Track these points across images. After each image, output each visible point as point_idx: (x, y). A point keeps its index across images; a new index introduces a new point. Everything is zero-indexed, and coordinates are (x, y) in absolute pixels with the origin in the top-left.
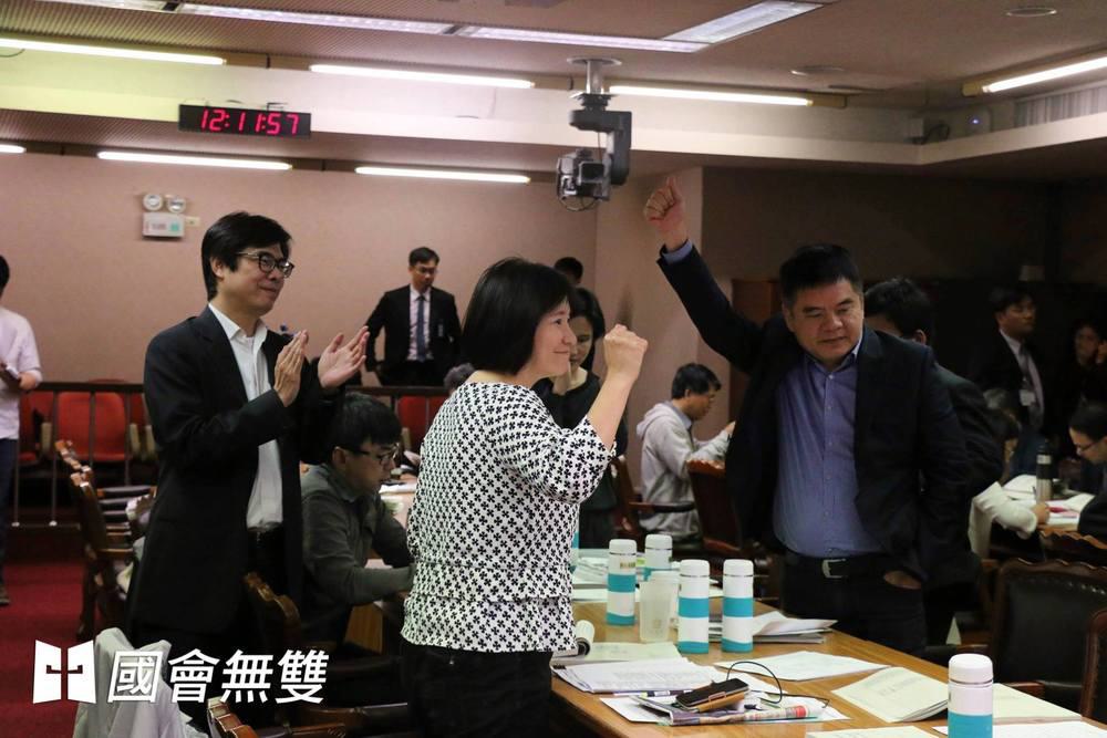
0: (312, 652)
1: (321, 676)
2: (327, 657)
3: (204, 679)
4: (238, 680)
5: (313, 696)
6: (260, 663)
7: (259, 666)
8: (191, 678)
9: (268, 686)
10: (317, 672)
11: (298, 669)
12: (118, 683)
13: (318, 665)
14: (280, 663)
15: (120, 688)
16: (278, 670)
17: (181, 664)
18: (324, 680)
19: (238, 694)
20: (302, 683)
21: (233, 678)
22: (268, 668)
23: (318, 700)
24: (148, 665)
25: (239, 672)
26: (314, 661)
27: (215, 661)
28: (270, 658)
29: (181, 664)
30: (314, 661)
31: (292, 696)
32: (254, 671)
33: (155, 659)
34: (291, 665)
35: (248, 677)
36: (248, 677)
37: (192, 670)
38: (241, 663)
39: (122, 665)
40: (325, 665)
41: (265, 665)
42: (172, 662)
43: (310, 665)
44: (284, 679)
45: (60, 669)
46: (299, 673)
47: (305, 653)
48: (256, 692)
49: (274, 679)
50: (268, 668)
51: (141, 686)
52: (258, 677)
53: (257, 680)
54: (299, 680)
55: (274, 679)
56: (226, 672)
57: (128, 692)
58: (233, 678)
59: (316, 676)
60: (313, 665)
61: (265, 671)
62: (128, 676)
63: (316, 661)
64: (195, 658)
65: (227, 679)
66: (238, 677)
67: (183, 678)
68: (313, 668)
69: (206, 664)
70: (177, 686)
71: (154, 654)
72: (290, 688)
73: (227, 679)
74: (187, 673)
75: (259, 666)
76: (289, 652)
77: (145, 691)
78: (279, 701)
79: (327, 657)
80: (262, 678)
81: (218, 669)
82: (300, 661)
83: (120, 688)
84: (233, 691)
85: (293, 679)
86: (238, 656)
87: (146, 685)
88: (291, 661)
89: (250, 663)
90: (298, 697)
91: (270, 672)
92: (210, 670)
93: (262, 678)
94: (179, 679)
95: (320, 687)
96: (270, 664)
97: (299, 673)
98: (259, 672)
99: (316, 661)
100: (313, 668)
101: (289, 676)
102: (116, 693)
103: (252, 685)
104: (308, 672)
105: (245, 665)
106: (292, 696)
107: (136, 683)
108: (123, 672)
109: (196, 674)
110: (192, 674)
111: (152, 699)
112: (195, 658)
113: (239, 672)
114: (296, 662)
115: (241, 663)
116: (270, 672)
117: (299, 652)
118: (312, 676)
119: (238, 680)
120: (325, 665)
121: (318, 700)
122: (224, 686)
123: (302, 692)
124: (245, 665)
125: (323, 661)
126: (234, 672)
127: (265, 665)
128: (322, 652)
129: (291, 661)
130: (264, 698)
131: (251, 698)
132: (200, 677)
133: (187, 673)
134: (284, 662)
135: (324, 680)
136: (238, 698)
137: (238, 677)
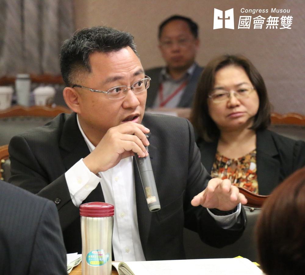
0: (289, 16)
1: (291, 22)
2: (292, 18)
3: (262, 23)
5: (289, 27)
6: (276, 19)
7: (276, 20)
8: (259, 23)
9: (278, 25)
10: (290, 21)
11: (285, 20)
12: (240, 24)
13: (290, 19)
14: (281, 19)
15: (241, 25)
16: (280, 21)
18: (292, 23)
19: (270, 27)
20: (286, 24)
21: (269, 23)
22: (278, 20)
23: (290, 28)
25: (271, 21)
26: (289, 18)
27: (265, 18)
28: (278, 18)
29: (256, 19)
30: (289, 18)
31: (284, 27)
32: (274, 21)
34: (283, 20)
35: (273, 22)
36: (273, 22)
37: (259, 21)
38: (271, 19)
40: (292, 19)
41: (277, 19)
42: (254, 19)
43: (288, 19)
44: (282, 23)
45: (225, 20)
46: (286, 21)
48: (275, 26)
49: (279, 23)
50: (278, 20)
51: (246, 25)
52: (275, 22)
53: (275, 23)
54: (285, 23)
55: (279, 23)
56: (267, 21)
57: (243, 26)
58: (269, 23)
59: (290, 22)
60: (289, 19)
61: (277, 21)
62: (243, 22)
63: (290, 18)
64: (260, 18)
65: (268, 23)
66: (270, 22)
67: (257, 23)
68: (289, 20)
69: (262, 19)
70: (255, 25)
72: (283, 25)
73: (268, 23)
74: (258, 22)
75: (276, 20)
76: (283, 16)
77: (247, 26)
78: (280, 28)
79: (292, 18)
80: (276, 23)
81: (265, 20)
82: (286, 18)
83: (241, 25)
84: (269, 26)
85: (284, 23)
86: (270, 17)
87: (247, 25)
88: (283, 18)
89: (273, 19)
90: (285, 27)
91: (278, 21)
92: (263, 21)
93: (276, 23)
95: (291, 25)
97: (286, 21)
98: (275, 21)
99: (290, 18)
100: (289, 20)
101: (283, 22)
102: (240, 27)
103: (274, 24)
104: (288, 21)
105: (272, 19)
106: (284, 27)
107: (245, 24)
108: (242, 21)
109: (260, 22)
110: (259, 22)
111: (249, 28)
112: (260, 18)
113: (271, 21)
114: (285, 18)
115: (271, 19)
116: (278, 21)
117: (285, 16)
118: (289, 22)
120: (292, 21)
121: (290, 28)
122: (267, 25)
124: (272, 19)
125: (291, 18)
126: (269, 21)
127: (277, 19)
128: (291, 16)
129: (283, 18)
130: (277, 28)
131: (273, 28)
132: (261, 23)
133: (258, 22)
134: (282, 19)
135: (292, 23)
136: (270, 28)
137: (270, 22)
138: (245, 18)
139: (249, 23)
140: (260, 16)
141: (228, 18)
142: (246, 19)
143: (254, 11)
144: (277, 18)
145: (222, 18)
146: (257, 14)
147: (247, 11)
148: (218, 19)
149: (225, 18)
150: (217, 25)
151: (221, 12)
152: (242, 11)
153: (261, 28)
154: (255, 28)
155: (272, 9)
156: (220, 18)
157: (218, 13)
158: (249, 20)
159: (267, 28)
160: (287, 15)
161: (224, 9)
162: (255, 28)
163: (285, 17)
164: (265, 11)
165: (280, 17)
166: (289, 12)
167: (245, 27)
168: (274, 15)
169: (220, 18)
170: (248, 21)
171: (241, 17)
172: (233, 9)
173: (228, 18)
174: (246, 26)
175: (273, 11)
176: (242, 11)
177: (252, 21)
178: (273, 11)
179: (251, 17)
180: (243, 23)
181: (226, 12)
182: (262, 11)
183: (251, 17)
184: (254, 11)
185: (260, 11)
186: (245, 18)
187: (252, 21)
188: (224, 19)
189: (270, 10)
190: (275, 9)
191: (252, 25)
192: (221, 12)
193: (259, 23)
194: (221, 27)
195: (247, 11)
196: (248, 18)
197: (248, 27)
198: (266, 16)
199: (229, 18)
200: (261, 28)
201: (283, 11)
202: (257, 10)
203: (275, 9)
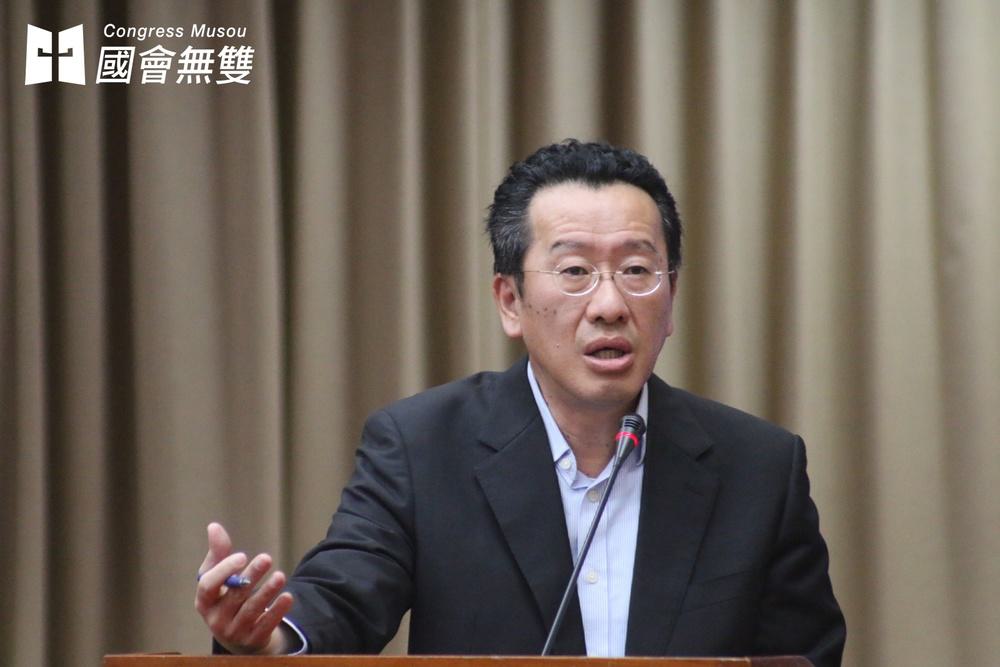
0: (243, 47)
1: (248, 65)
2: (253, 51)
4: (189, 68)
6: (205, 55)
7: (205, 58)
8: (156, 66)
9: (211, 72)
10: (246, 62)
11: (233, 59)
12: (103, 70)
13: (247, 56)
14: (219, 55)
15: (105, 74)
16: (218, 61)
17: (148, 56)
18: (251, 68)
19: (189, 78)
20: (235, 70)
21: (186, 67)
23: (247, 82)
24: (123, 56)
25: (190, 61)
26: (244, 54)
27: (173, 54)
28: (212, 51)
29: (148, 56)
30: (244, 54)
32: (200, 61)
33: (129, 52)
35: (196, 65)
36: (196, 65)
37: (156, 60)
38: (191, 55)
39: (107, 56)
40: (251, 56)
41: (208, 56)
42: (142, 55)
44: (222, 67)
45: (60, 58)
47: (238, 48)
48: (202, 76)
49: (215, 67)
51: (119, 72)
52: (203, 65)
53: (203, 68)
54: (233, 68)
55: (215, 67)
56: (180, 61)
57: (109, 77)
58: (186, 67)
59: (245, 65)
60: (243, 56)
61: (209, 61)
62: (110, 65)
63: (245, 53)
65: (181, 66)
66: (189, 65)
67: (150, 66)
68: (243, 59)
69: (166, 56)
70: (145, 72)
72: (227, 73)
73: (181, 66)
74: (153, 63)
75: (205, 58)
76: (226, 47)
77: (123, 75)
78: (219, 82)
79: (253, 51)
80: (207, 67)
82: (234, 54)
83: (105, 74)
84: (186, 75)
85: (229, 67)
86: (189, 50)
88: (227, 54)
89: (198, 55)
90: (232, 80)
91: (212, 61)
92: (169, 60)
93: (207, 67)
94: (147, 67)
95: (248, 72)
96: (212, 56)
98: (204, 61)
100: (243, 59)
101: (225, 65)
102: (102, 77)
103: (199, 71)
104: (239, 62)
105: (194, 56)
107: (116, 70)
108: (107, 62)
110: (156, 63)
113: (190, 61)
114: (231, 54)
115: (191, 55)
116: (212, 61)
117: (233, 48)
118: (242, 65)
119: (189, 68)
120: (251, 56)
121: (247, 82)
122: (179, 71)
123: (235, 76)
124: (194, 56)
126: (186, 62)
128: (249, 48)
129: (227, 54)
130: (207, 80)
131: (198, 81)
132: (162, 66)
133: (153, 63)
134: (222, 54)
135: (251, 68)
136: (189, 81)
137: (189, 65)
138: (116, 52)
139: (126, 68)
140: (159, 47)
141: (66, 51)
142: (119, 56)
143: (142, 32)
149: (60, 52)
150: (37, 72)
151: (48, 35)
152: (110, 31)
153: (163, 81)
155: (195, 26)
156: (44, 51)
157: (37, 38)
158: (128, 60)
159: (179, 81)
160: (236, 43)
161: (54, 25)
162: (144, 81)
164: (175, 32)
165: (218, 51)
166: (244, 35)
167: (116, 77)
169: (44, 51)
172: (81, 26)
173: (66, 51)
174: (118, 77)
176: (110, 31)
177: (138, 60)
179: (133, 49)
181: (62, 35)
182: (166, 32)
184: (142, 32)
185: (160, 32)
186: (116, 52)
187: (138, 60)
188: (55, 55)
189: (188, 31)
190: (204, 26)
191: (137, 73)
194: (48, 78)
196: (126, 53)
197: (125, 77)
198: (178, 46)
199: (70, 53)
200: (163, 81)
201: (225, 32)
202: (151, 29)
203: (204, 26)
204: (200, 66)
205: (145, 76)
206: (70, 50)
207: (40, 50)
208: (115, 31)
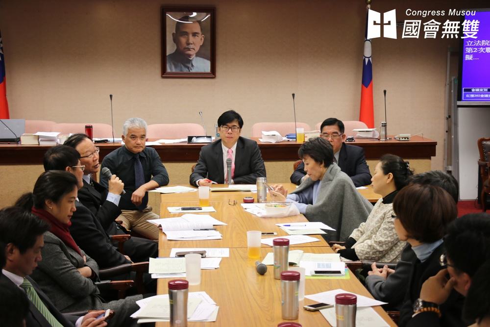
0: (474, 20)
1: (477, 29)
2: (479, 22)
4: (448, 30)
5: (474, 36)
6: (455, 24)
8: (431, 30)
9: (458, 32)
10: (475, 28)
12: (405, 32)
13: (476, 25)
15: (406, 33)
16: (462, 27)
17: (428, 25)
18: (478, 30)
19: (448, 35)
20: (470, 31)
21: (446, 30)
23: (476, 37)
25: (448, 27)
26: (474, 24)
27: (439, 24)
28: (459, 22)
29: (428, 25)
30: (474, 24)
32: (453, 27)
33: (418, 23)
35: (451, 29)
36: (451, 29)
37: (431, 27)
38: (449, 24)
39: (407, 25)
40: (478, 25)
41: (457, 25)
42: (424, 24)
44: (464, 30)
45: (384, 26)
46: (469, 28)
47: (471, 21)
48: (454, 35)
49: (461, 30)
51: (414, 32)
53: (454, 31)
54: (469, 30)
55: (461, 30)
56: (443, 27)
57: (409, 35)
58: (446, 30)
61: (457, 27)
62: (409, 29)
63: (475, 24)
64: (433, 22)
65: (444, 30)
66: (448, 29)
67: (428, 29)
68: (474, 26)
69: (437, 25)
70: (426, 33)
71: (418, 21)
72: (466, 33)
73: (444, 30)
74: (430, 28)
76: (466, 20)
77: (415, 34)
78: (462, 38)
79: (479, 22)
80: (456, 30)
81: (441, 26)
82: (469, 24)
83: (406, 33)
84: (446, 34)
85: (467, 30)
86: (448, 22)
88: (466, 24)
89: (452, 24)
90: (469, 36)
91: (459, 27)
92: (438, 27)
93: (456, 30)
94: (427, 30)
95: (476, 33)
97: (469, 28)
98: (455, 27)
99: (475, 24)
100: (474, 26)
101: (465, 29)
102: (405, 35)
103: (453, 32)
104: (472, 27)
105: (450, 25)
107: (412, 31)
108: (407, 28)
109: (433, 28)
110: (431, 28)
111: (417, 37)
112: (433, 22)
113: (448, 27)
114: (468, 24)
115: (449, 24)
116: (459, 27)
117: (469, 21)
118: (474, 29)
119: (448, 30)
120: (478, 25)
121: (476, 37)
122: (443, 32)
123: (470, 34)
124: (450, 25)
125: (477, 26)
126: (446, 28)
127: (457, 25)
128: (477, 21)
129: (466, 24)
130: (457, 37)
131: (452, 37)
132: (434, 29)
133: (430, 28)
134: (464, 24)
135: (478, 30)
136: (448, 37)
137: (448, 29)
138: (412, 23)
139: (417, 30)
140: (433, 20)
142: (413, 25)
143: (425, 13)
144: (458, 23)
145: (380, 23)
146: (429, 18)
147: (415, 13)
148: (374, 24)
149: (385, 22)
150: (373, 32)
151: (379, 14)
152: (408, 14)
153: (435, 37)
154: (426, 37)
155: (450, 10)
157: (373, 16)
158: (418, 26)
159: (443, 37)
160: (471, 18)
161: (382, 11)
162: (426, 37)
163: (469, 21)
164: (441, 13)
165: (462, 22)
166: (474, 14)
168: (453, 18)
170: (416, 28)
171: (406, 21)
174: (413, 35)
175: (452, 12)
176: (408, 14)
177: (422, 27)
178: (452, 12)
179: (420, 21)
180: (409, 30)
181: (385, 14)
182: (436, 13)
183: (420, 21)
184: (425, 13)
185: (433, 13)
186: (412, 23)
187: (422, 27)
188: (382, 24)
189: (447, 12)
190: (455, 10)
191: (422, 33)
192: (380, 14)
193: (431, 30)
194: (379, 36)
195: (414, 13)
196: (417, 23)
197: (416, 35)
198: (442, 20)
199: (389, 23)
200: (435, 37)
202: (429, 12)
203: (455, 10)
204: (453, 30)
205: (426, 34)
206: (389, 22)
207: (375, 22)
208: (411, 12)
